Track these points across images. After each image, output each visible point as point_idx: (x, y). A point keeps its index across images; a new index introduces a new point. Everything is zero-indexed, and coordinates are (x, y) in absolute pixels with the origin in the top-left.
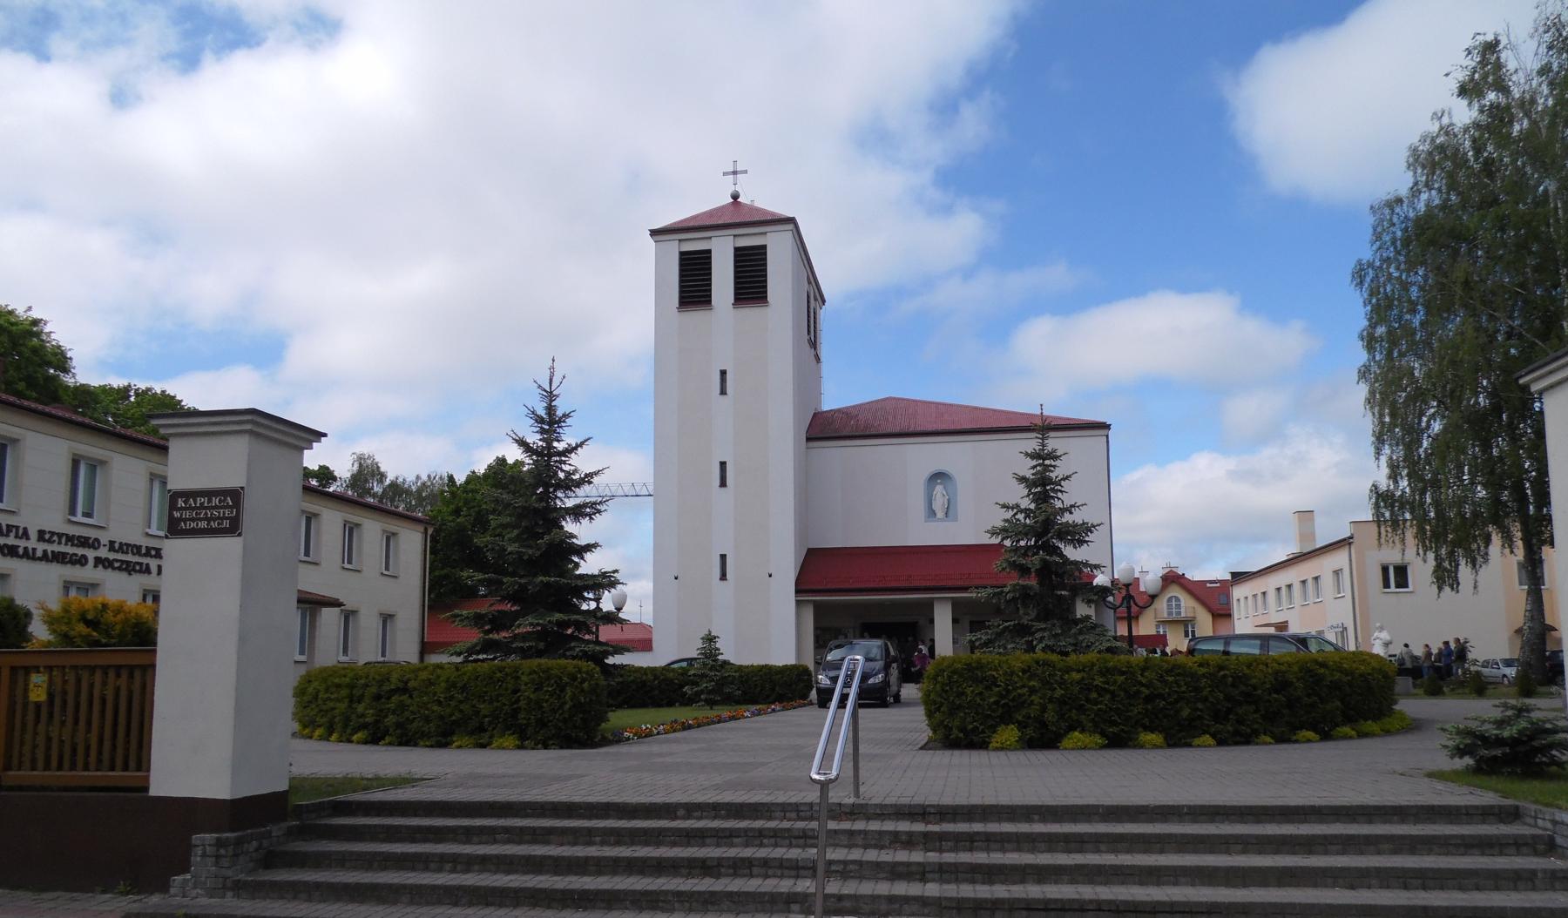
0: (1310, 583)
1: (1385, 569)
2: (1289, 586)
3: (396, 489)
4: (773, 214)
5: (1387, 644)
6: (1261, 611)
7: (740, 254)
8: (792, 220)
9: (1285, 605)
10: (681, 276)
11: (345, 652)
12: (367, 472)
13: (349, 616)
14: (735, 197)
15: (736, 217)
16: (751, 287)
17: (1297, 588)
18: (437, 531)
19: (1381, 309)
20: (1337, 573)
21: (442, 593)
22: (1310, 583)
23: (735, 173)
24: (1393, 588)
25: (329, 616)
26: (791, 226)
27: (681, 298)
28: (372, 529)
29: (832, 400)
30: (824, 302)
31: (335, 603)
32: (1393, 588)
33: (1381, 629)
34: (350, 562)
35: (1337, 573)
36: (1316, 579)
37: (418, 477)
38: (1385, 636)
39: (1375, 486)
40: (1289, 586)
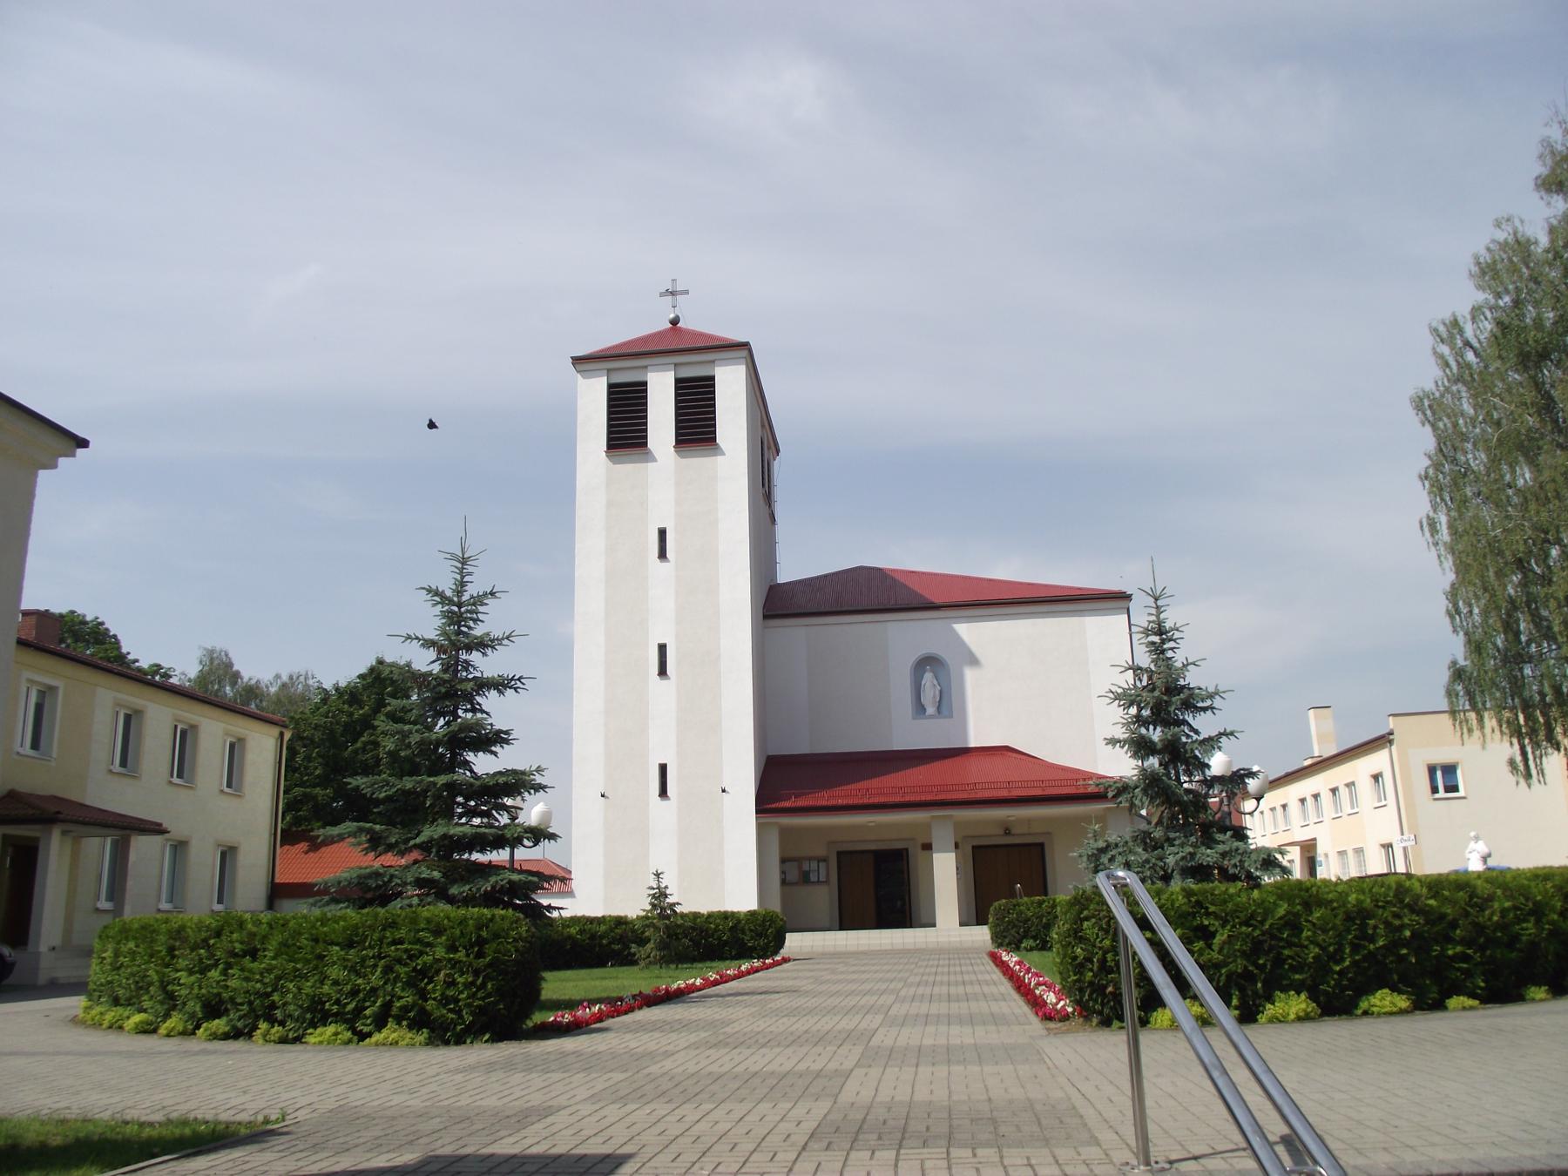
0: (1343, 792)
1: (1432, 770)
2: (1316, 796)
3: (252, 692)
4: (718, 338)
5: (1485, 859)
6: (1313, 818)
7: (680, 384)
8: (745, 346)
9: (1313, 818)
10: (609, 413)
11: (220, 901)
12: (219, 669)
13: (180, 847)
14: (675, 322)
15: (674, 343)
16: (696, 428)
17: (1326, 797)
18: (297, 737)
19: (1448, 447)
20: (1376, 777)
21: (300, 820)
22: (1310, 801)
23: (673, 293)
24: (1442, 794)
25: (143, 848)
26: (745, 353)
27: (609, 439)
28: (214, 730)
29: (789, 571)
30: (778, 451)
31: (156, 829)
32: (1442, 794)
33: (1477, 839)
34: (180, 776)
35: (1376, 777)
36: (1284, 806)
37: (278, 676)
38: (1481, 847)
39: (1454, 663)
40: (1316, 796)
